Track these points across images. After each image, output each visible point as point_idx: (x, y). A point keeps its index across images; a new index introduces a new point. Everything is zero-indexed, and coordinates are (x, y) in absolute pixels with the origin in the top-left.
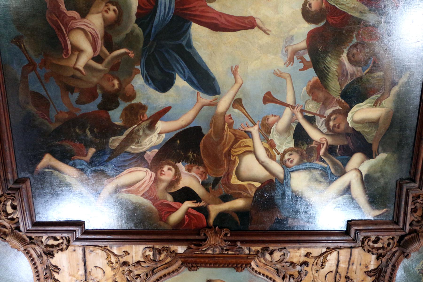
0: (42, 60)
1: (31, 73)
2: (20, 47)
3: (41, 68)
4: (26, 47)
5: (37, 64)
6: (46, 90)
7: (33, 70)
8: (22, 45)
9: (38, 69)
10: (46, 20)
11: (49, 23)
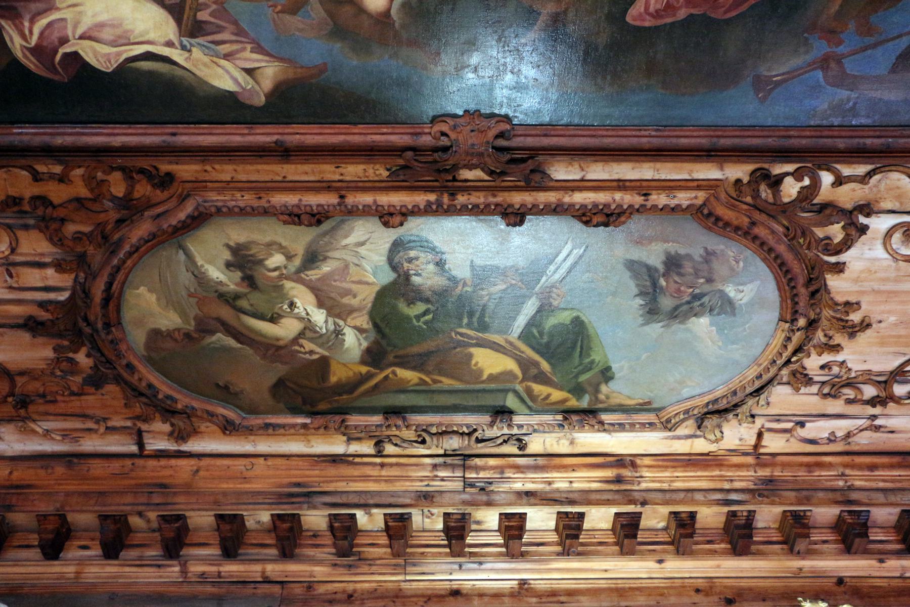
0: (820, 38)
1: (846, 66)
2: (778, 84)
3: (840, 43)
4: (781, 72)
5: (829, 50)
6: (899, 36)
7: (839, 62)
8: (774, 79)
9: (841, 49)
10: (730, 19)
11: (738, 13)
